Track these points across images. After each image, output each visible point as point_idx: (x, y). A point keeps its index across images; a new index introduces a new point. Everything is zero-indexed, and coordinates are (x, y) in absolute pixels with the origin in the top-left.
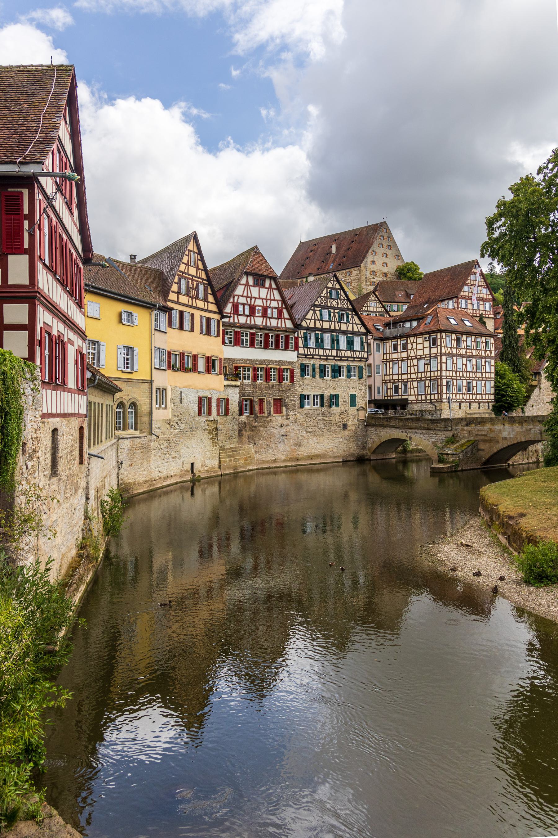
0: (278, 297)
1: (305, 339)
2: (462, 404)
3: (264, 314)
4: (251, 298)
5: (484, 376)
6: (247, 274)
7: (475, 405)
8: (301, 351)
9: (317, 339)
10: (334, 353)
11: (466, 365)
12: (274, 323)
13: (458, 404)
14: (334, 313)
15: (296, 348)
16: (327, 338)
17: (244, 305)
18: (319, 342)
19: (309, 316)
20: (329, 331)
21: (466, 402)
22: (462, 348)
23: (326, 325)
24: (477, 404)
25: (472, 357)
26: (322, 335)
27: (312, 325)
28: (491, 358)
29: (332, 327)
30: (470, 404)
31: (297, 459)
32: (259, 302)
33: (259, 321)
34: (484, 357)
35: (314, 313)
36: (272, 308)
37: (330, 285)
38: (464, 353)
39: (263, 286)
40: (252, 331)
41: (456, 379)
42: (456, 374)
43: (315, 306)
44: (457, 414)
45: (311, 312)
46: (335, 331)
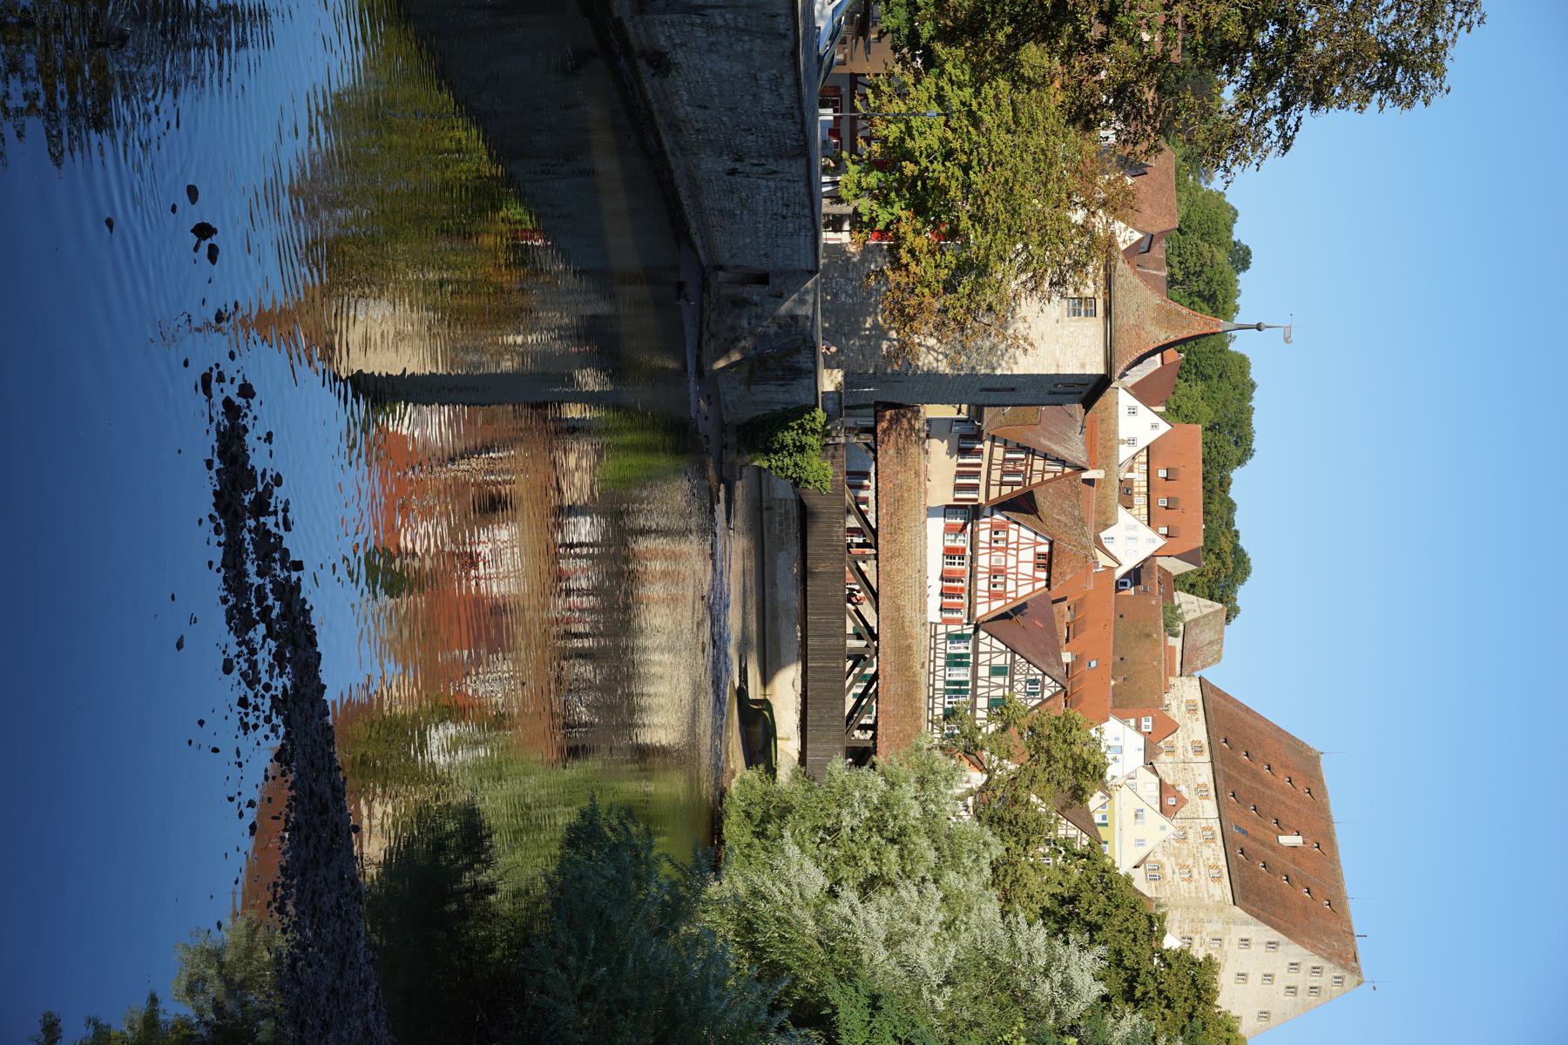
0: (1025, 590)
1: (960, 638)
3: (995, 572)
4: (1018, 550)
6: (1051, 544)
8: (941, 629)
9: (961, 656)
10: (940, 685)
12: (982, 584)
14: (1003, 687)
15: (946, 622)
16: (961, 674)
17: (1007, 539)
18: (955, 661)
19: (996, 643)
20: (975, 677)
23: (983, 671)
26: (967, 665)
27: (982, 648)
29: (980, 683)
31: (775, 618)
32: (1011, 561)
33: (983, 561)
35: (1002, 652)
36: (1005, 584)
37: (1048, 680)
39: (1037, 566)
40: (968, 552)
43: (1014, 652)
45: (1003, 647)
46: (975, 686)
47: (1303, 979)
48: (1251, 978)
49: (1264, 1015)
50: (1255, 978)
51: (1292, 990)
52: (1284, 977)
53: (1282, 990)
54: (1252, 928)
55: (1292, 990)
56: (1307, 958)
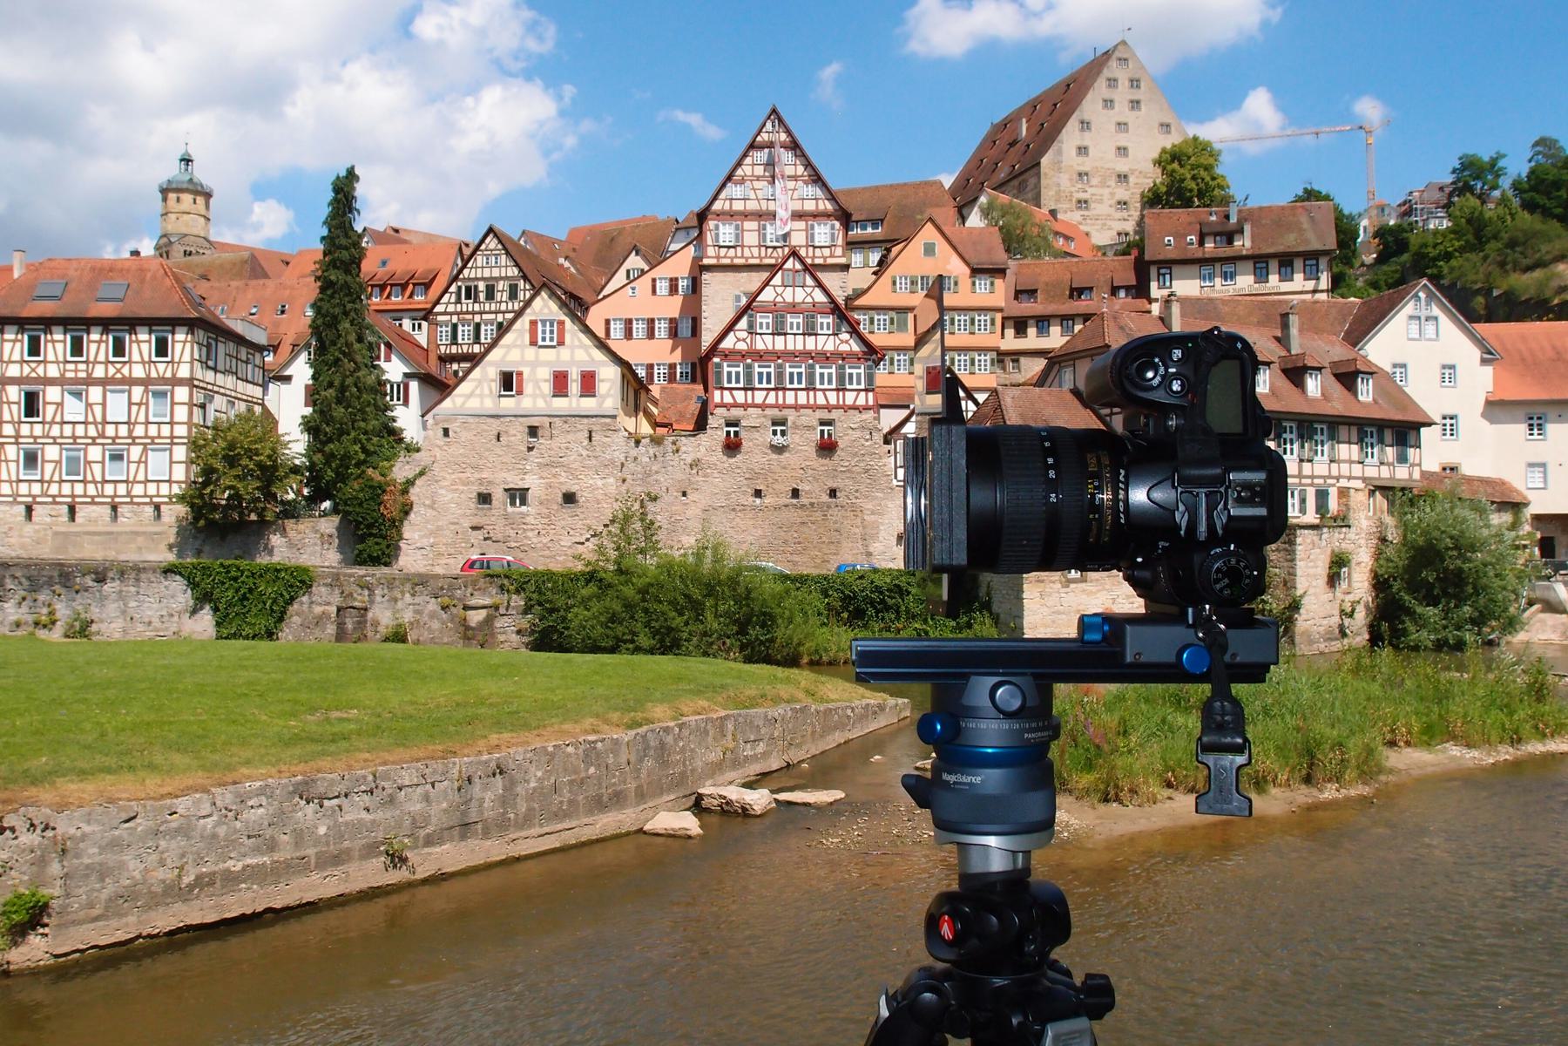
2: (37, 509)
5: (139, 431)
7: (93, 516)
11: (60, 405)
13: (22, 508)
21: (55, 503)
22: (45, 362)
24: (107, 510)
25: (90, 381)
28: (176, 381)
30: (72, 510)
34: (145, 382)
38: (53, 371)
41: (17, 443)
42: (17, 431)
44: (15, 533)
47: (1122, 94)
48: (1122, 144)
49: (1166, 127)
50: (1122, 140)
51: (1135, 104)
52: (1121, 111)
53: (1136, 113)
54: (1064, 146)
55: (1135, 104)
56: (1100, 89)
